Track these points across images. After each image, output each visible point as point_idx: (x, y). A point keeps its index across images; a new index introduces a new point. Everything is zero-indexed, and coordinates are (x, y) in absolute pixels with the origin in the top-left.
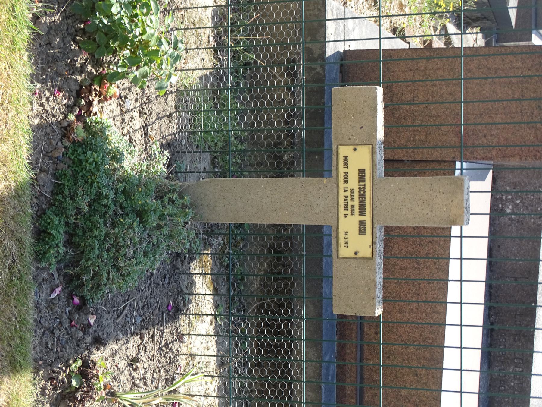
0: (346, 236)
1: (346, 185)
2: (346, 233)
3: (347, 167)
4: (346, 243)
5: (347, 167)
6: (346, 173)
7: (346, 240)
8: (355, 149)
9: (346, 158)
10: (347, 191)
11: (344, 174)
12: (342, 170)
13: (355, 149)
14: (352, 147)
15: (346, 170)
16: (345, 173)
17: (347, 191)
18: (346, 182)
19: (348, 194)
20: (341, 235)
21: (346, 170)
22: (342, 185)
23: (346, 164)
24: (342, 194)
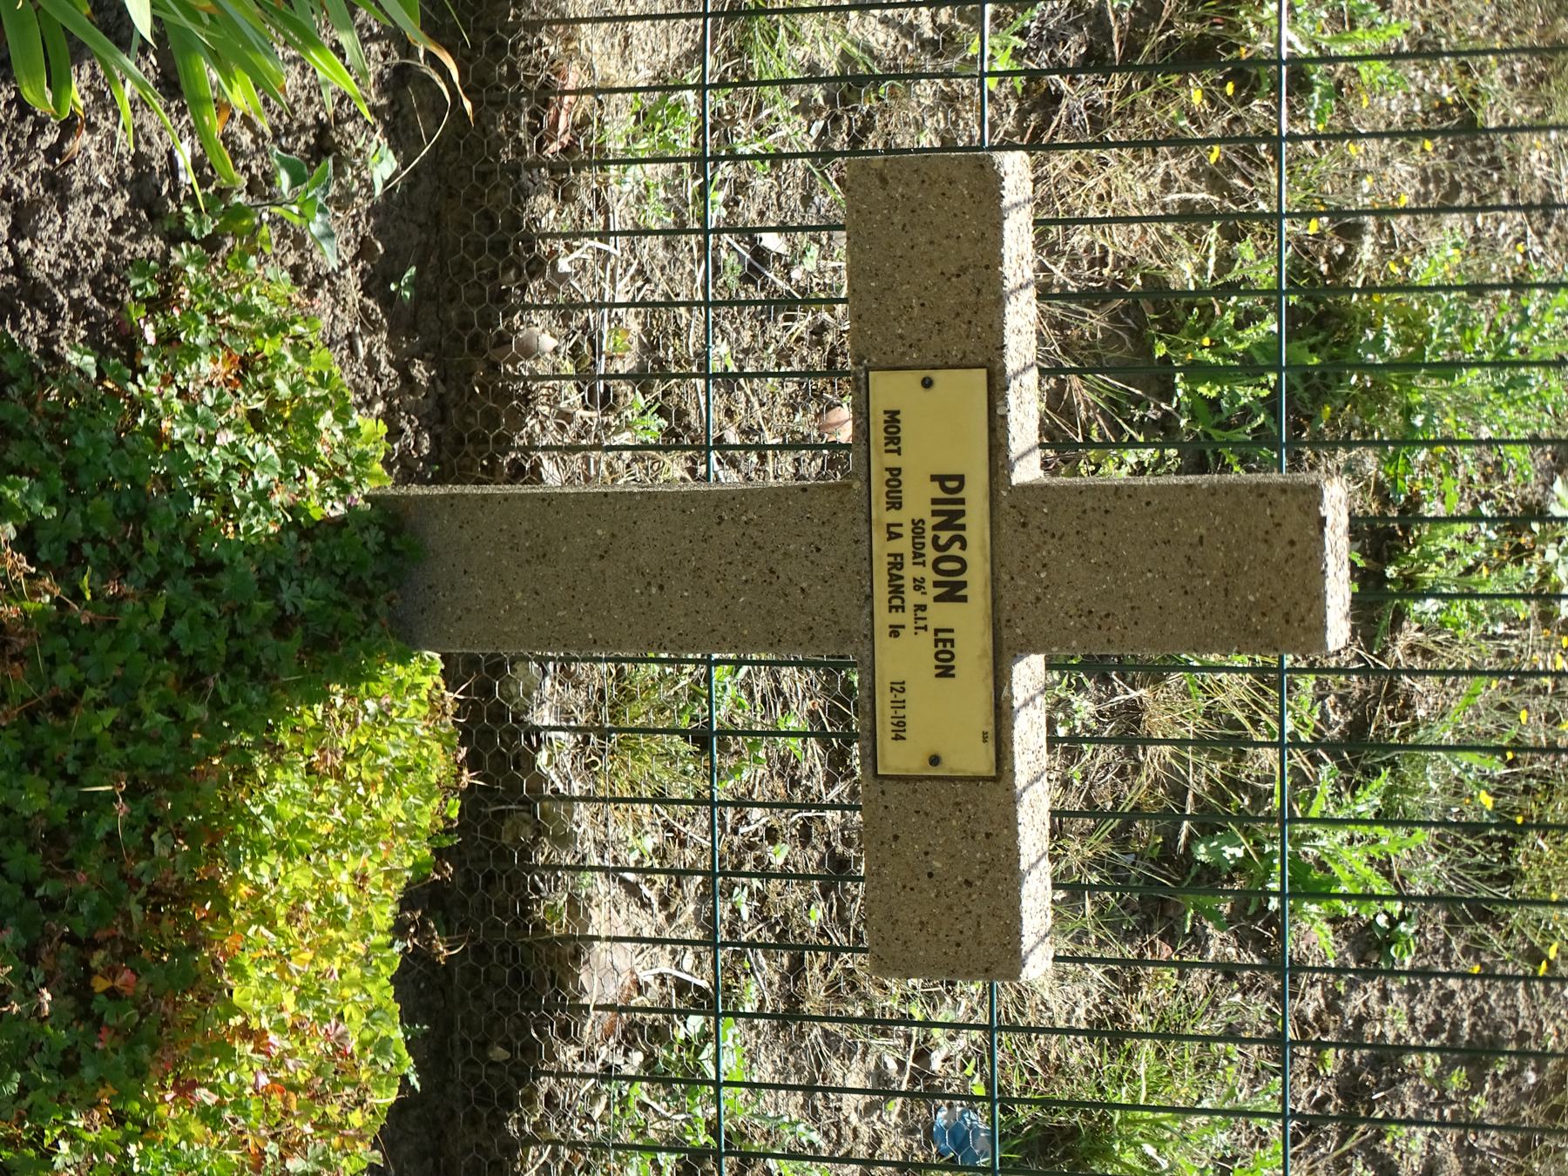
0: (901, 697)
1: (893, 516)
2: (899, 687)
3: (898, 451)
4: (900, 725)
5: (898, 451)
6: (895, 472)
7: (901, 712)
8: (927, 384)
9: (893, 418)
10: (899, 536)
11: (887, 475)
12: (881, 461)
13: (927, 384)
14: (915, 377)
15: (892, 460)
16: (889, 470)
17: (899, 536)
18: (895, 503)
19: (904, 546)
20: (884, 700)
21: (892, 460)
22: (882, 515)
23: (893, 439)
24: (882, 548)
